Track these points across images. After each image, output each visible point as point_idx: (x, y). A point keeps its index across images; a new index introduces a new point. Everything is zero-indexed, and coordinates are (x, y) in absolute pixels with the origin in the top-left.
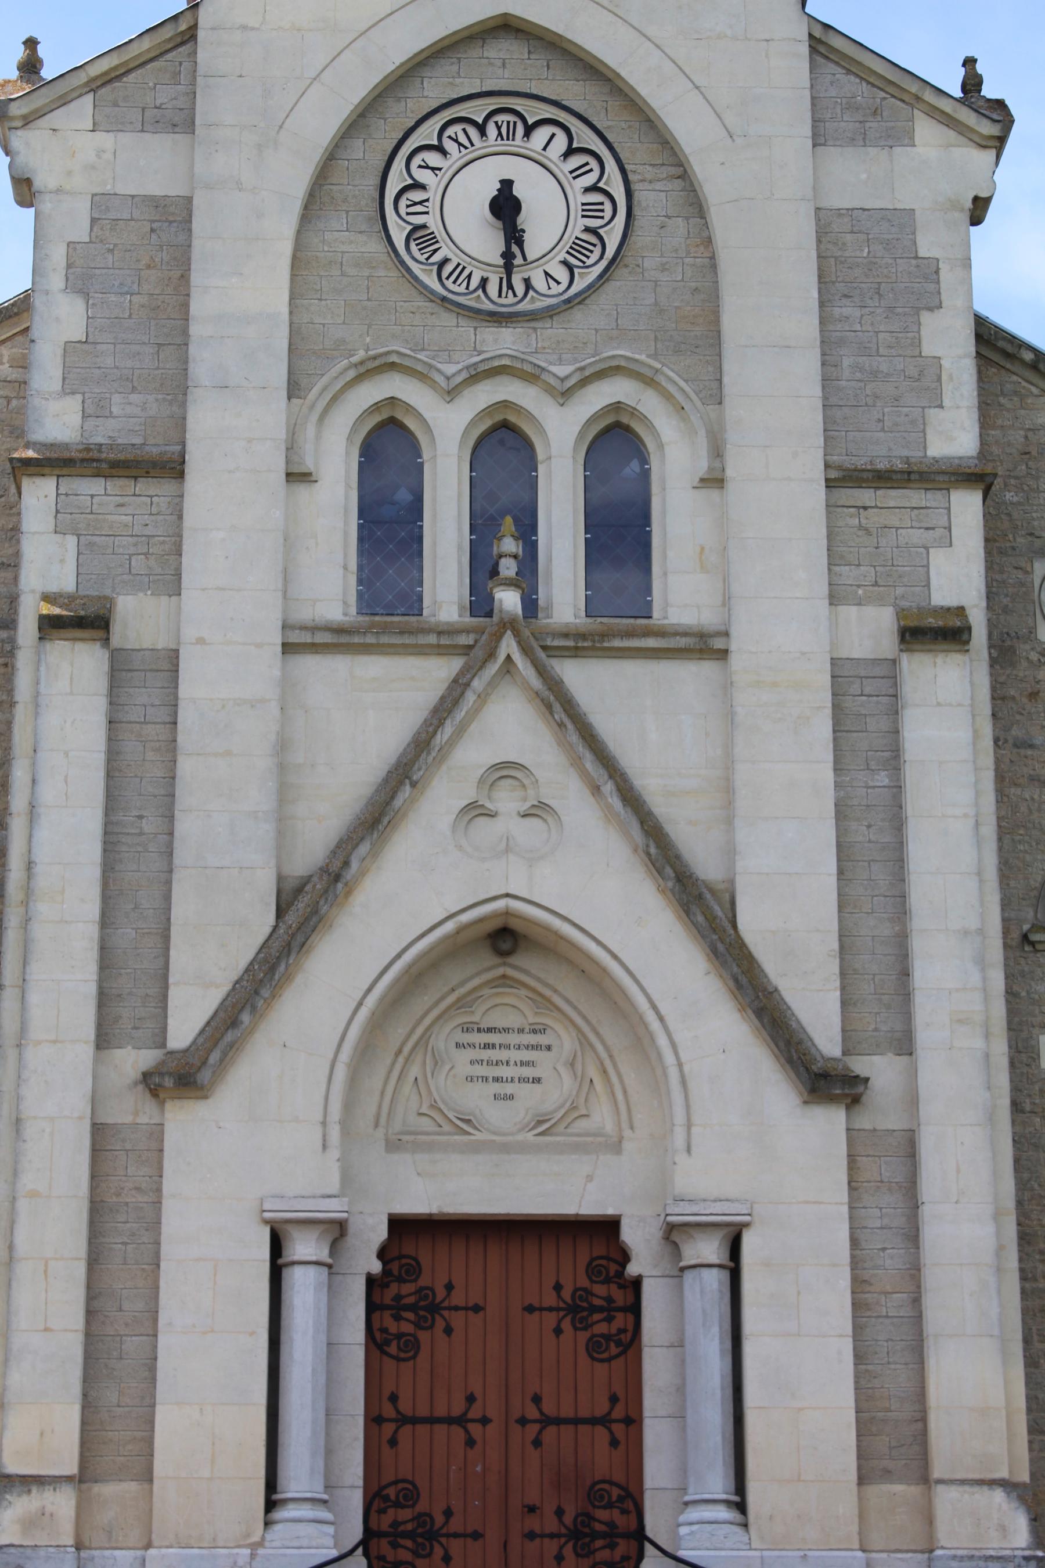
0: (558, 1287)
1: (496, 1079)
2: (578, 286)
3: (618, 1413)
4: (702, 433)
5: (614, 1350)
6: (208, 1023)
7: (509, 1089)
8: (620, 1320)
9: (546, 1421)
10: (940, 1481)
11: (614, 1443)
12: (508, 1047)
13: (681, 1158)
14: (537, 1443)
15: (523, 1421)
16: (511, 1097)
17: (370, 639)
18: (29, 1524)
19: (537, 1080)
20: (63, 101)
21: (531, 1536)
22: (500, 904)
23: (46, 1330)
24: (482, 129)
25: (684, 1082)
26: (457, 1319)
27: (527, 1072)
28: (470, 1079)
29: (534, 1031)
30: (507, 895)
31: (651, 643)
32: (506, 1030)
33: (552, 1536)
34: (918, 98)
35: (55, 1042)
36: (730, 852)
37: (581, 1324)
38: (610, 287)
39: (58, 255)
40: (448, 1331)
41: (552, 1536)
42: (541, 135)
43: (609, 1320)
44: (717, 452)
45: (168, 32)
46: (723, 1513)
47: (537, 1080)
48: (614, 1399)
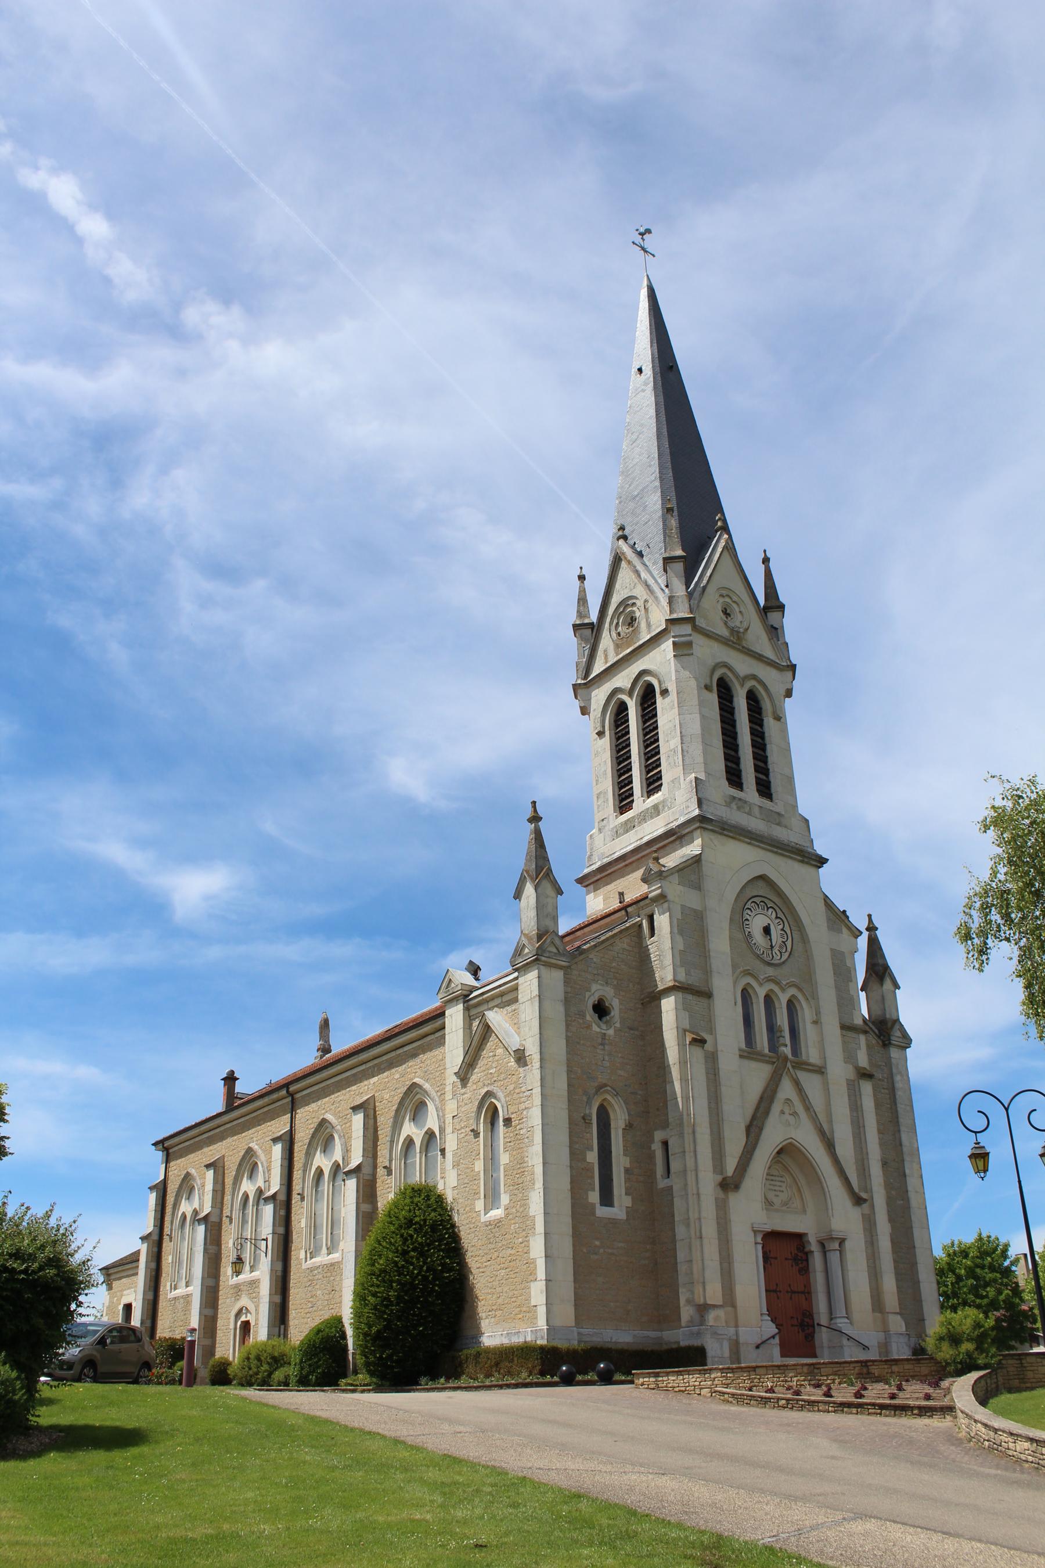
0: (791, 1253)
1: (775, 1190)
2: (785, 957)
3: (806, 1291)
4: (814, 1008)
5: (804, 1272)
6: (736, 1169)
7: (777, 1193)
8: (805, 1263)
9: (793, 1292)
10: (888, 1313)
11: (806, 1299)
12: (776, 1181)
13: (832, 1219)
14: (791, 1298)
15: (787, 1292)
16: (778, 1196)
17: (755, 1056)
18: (717, 1318)
19: (783, 1191)
20: (672, 874)
21: (792, 1325)
22: (790, 1140)
23: (712, 1260)
24: (768, 908)
25: (830, 1198)
26: (773, 1261)
27: (781, 1189)
28: (770, 1189)
29: (781, 1177)
30: (791, 1138)
31: (810, 1068)
32: (775, 1176)
33: (797, 1326)
34: (843, 921)
35: (705, 1171)
36: (832, 1132)
37: (797, 1264)
38: (789, 960)
39: (675, 921)
40: (771, 1264)
41: (797, 1326)
42: (770, 910)
43: (802, 1263)
44: (818, 1013)
45: (694, 859)
46: (846, 1320)
47: (783, 1191)
48: (805, 1286)
